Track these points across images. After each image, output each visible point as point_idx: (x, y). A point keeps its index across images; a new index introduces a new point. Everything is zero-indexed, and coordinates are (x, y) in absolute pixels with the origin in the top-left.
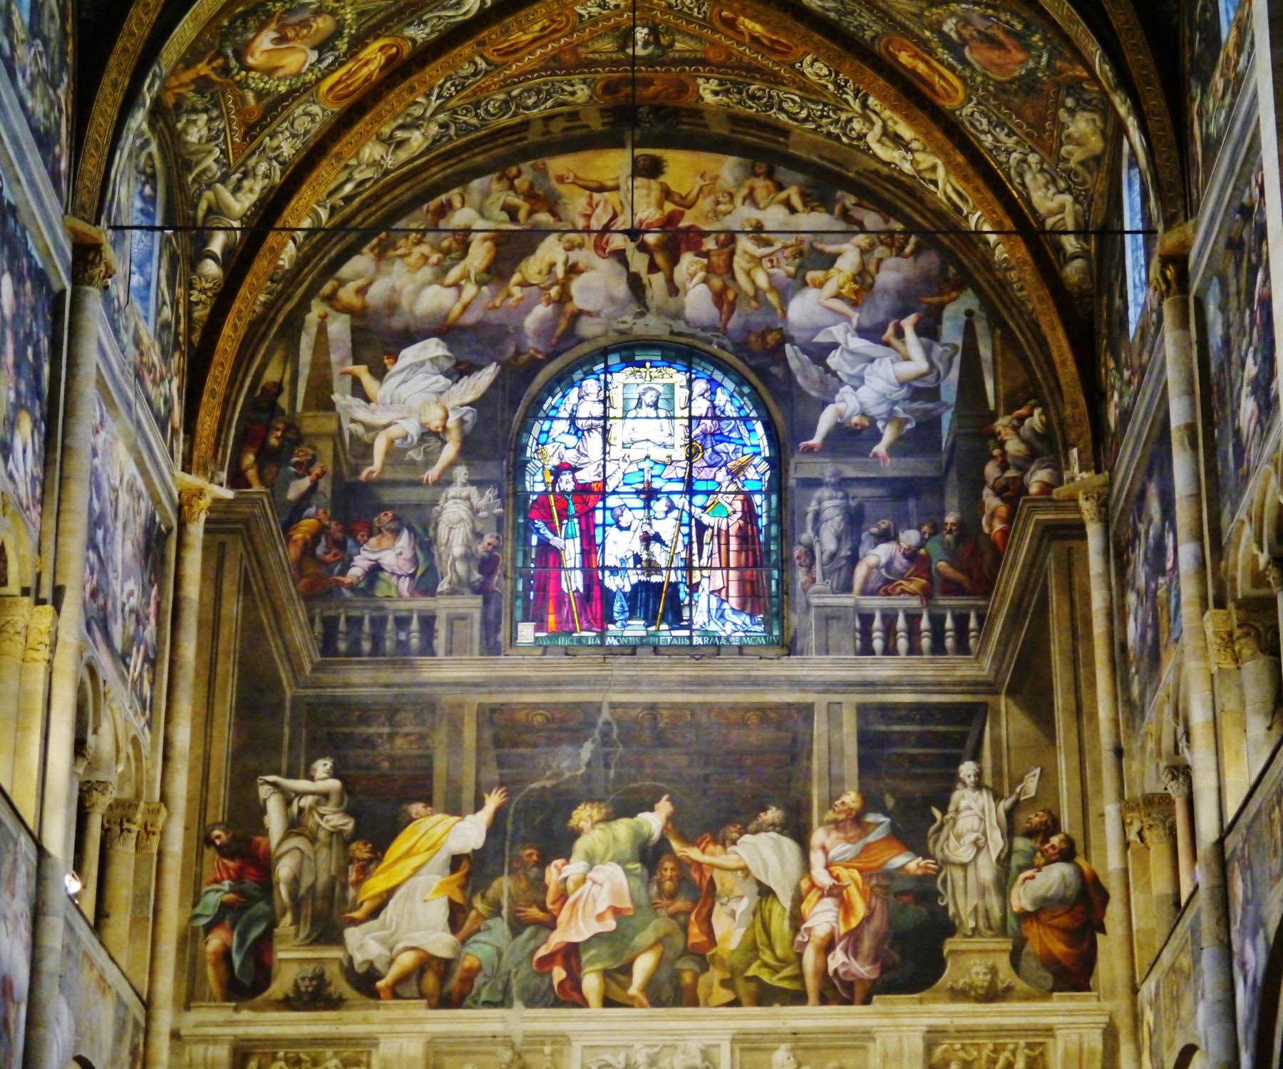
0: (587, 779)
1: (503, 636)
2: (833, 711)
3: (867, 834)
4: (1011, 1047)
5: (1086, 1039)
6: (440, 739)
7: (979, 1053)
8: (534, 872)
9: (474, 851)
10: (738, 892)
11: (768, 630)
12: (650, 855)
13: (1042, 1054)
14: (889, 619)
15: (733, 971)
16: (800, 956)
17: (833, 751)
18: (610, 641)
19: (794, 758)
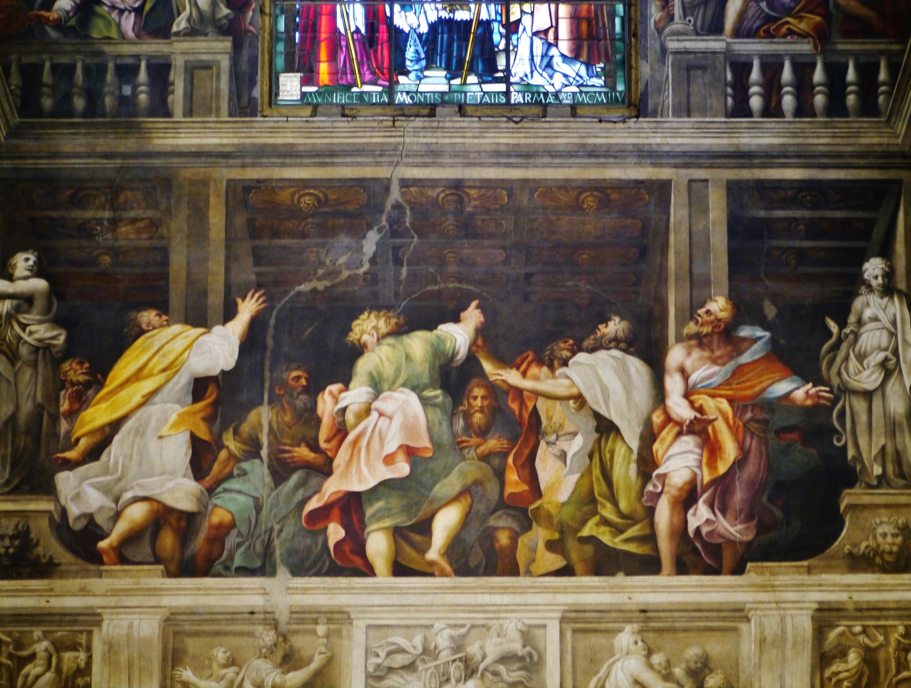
0: (372, 278)
1: (259, 91)
2: (696, 192)
3: (740, 353)
6: (178, 225)
8: (302, 401)
9: (223, 372)
10: (569, 427)
11: (610, 84)
12: (452, 378)
14: (771, 67)
15: (562, 529)
16: (651, 511)
17: (697, 245)
18: (400, 98)
19: (644, 253)
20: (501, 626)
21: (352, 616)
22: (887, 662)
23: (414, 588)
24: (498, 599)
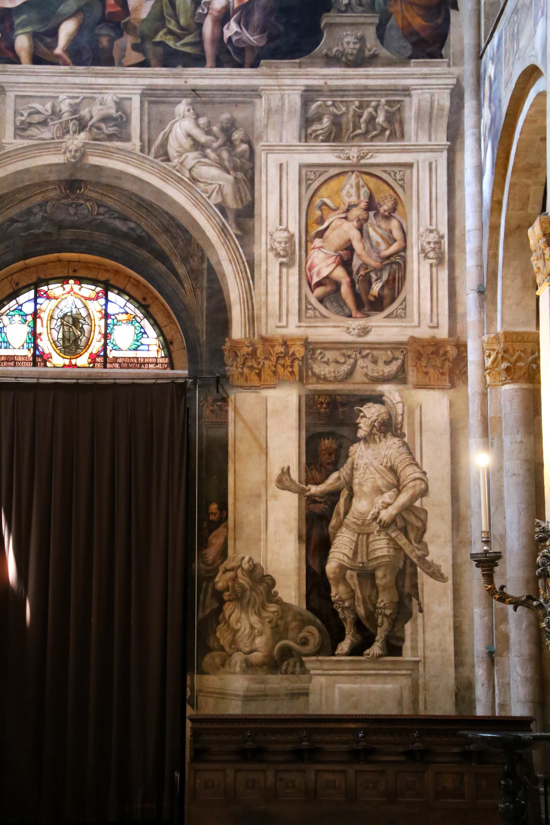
4: (373, 104)
5: (436, 97)
7: (347, 109)
13: (399, 109)
15: (143, 38)
16: (200, 26)
20: (103, 98)
21: (6, 89)
22: (348, 123)
23: (47, 72)
24: (101, 81)
